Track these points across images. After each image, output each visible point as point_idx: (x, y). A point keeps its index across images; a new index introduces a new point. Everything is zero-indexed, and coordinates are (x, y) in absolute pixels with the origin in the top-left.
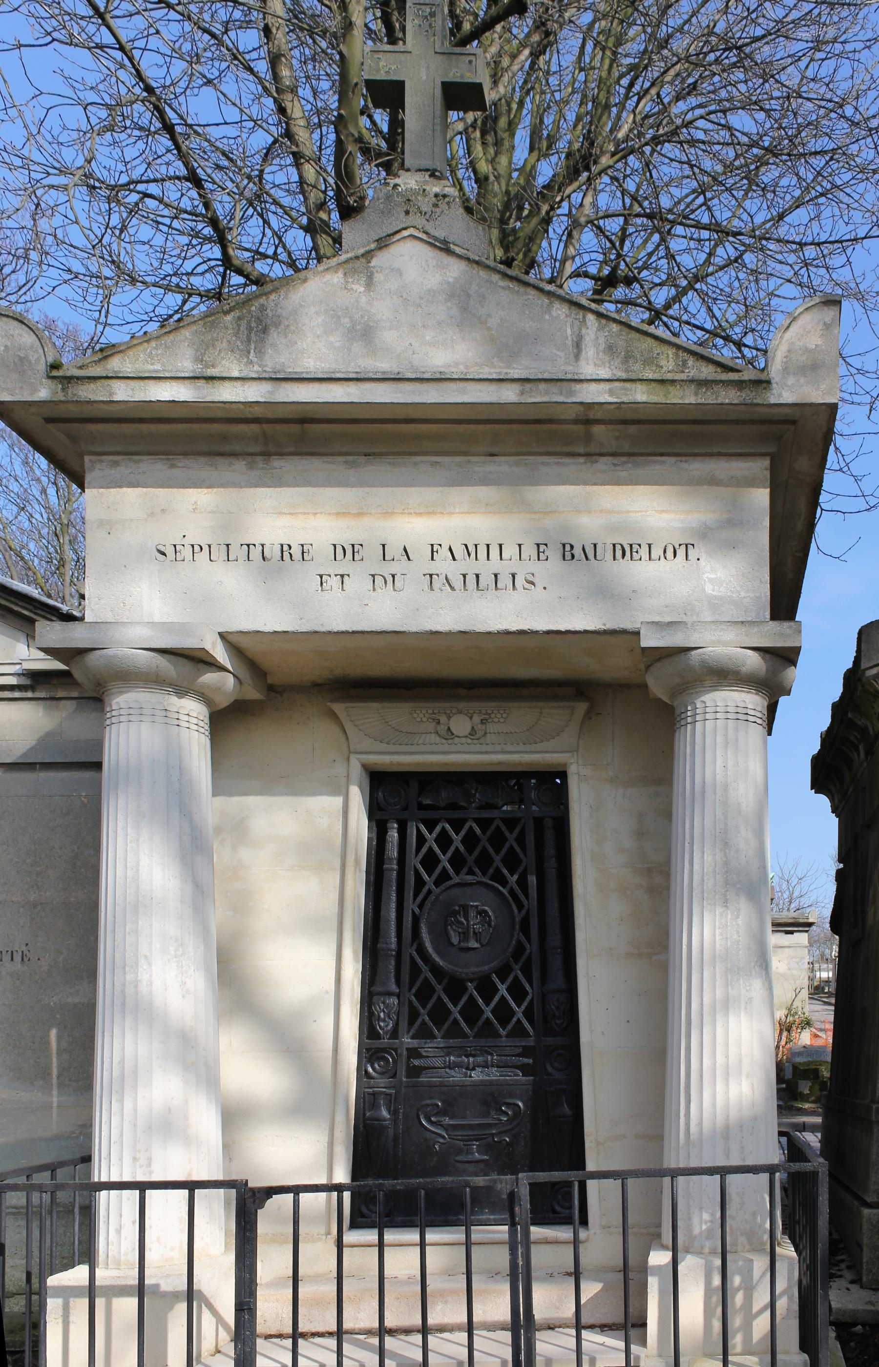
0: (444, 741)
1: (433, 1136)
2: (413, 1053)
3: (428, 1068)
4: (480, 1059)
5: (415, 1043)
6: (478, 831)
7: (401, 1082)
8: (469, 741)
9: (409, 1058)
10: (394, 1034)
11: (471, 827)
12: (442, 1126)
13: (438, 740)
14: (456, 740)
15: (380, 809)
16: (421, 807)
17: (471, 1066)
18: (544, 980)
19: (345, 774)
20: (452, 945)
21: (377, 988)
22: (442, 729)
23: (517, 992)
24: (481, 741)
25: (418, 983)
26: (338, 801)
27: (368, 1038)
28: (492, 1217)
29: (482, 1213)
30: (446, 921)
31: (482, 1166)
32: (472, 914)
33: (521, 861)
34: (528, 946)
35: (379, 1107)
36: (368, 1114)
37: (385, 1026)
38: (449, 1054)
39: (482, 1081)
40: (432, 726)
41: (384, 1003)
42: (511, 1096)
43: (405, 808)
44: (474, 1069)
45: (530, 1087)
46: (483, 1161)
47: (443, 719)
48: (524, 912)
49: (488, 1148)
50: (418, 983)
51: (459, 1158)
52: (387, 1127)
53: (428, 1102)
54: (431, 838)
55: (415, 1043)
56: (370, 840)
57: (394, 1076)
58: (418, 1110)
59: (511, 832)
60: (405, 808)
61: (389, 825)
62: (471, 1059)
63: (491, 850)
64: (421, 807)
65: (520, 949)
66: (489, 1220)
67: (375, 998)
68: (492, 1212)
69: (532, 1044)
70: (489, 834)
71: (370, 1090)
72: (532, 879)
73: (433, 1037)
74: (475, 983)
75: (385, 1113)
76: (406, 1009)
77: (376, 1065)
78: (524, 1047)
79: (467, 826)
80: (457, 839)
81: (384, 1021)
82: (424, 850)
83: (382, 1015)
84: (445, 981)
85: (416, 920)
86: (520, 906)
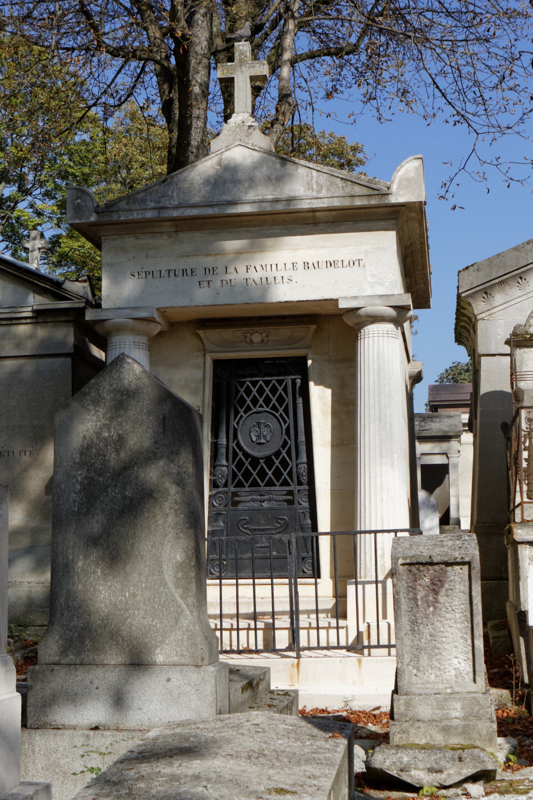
2: (235, 494)
4: (266, 497)
20: (253, 441)
22: (248, 340)
32: (262, 426)
34: (289, 441)
38: (251, 495)
44: (264, 502)
47: (249, 335)
48: (287, 425)
51: (257, 545)
53: (243, 518)
65: (285, 443)
84: (250, 459)
86: (285, 422)
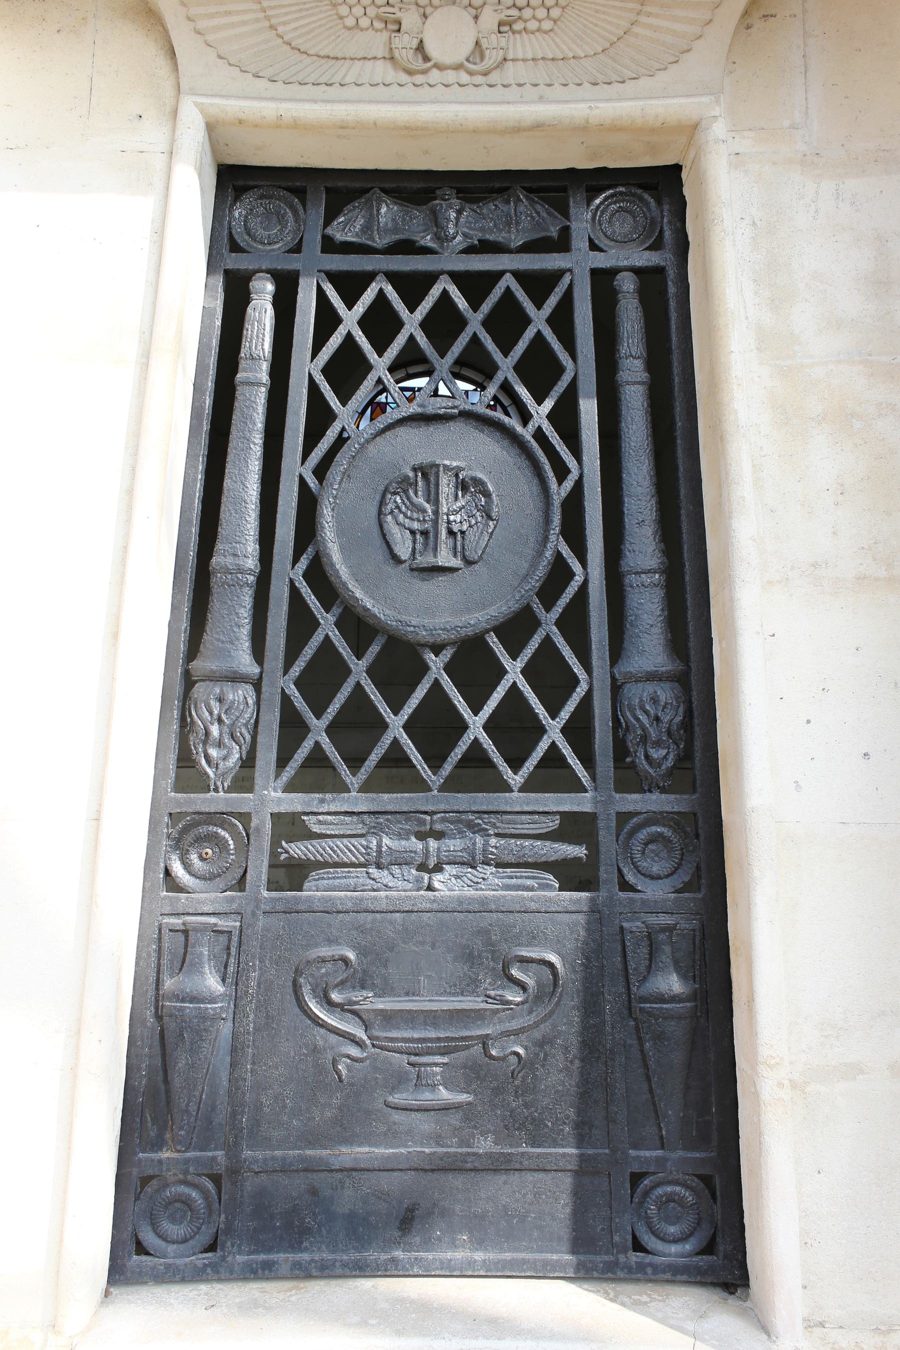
0: (404, 78)
1: (333, 1038)
2: (290, 826)
3: (326, 865)
4: (453, 845)
5: (295, 802)
6: (462, 303)
7: (258, 901)
8: (464, 78)
9: (275, 843)
10: (244, 778)
11: (445, 292)
12: (355, 1013)
13: (392, 75)
14: (435, 76)
15: (235, 247)
16: (329, 246)
17: (432, 863)
18: (617, 650)
19: (164, 147)
20: (397, 560)
21: (199, 665)
22: (405, 43)
23: (550, 677)
24: (494, 77)
25: (309, 652)
26: (148, 204)
27: (178, 788)
28: (479, 1256)
29: (454, 1245)
30: (382, 503)
31: (455, 1119)
32: (446, 486)
33: (560, 370)
34: (576, 567)
35: (197, 968)
36: (169, 984)
37: (221, 758)
38: (377, 830)
39: (460, 901)
40: (377, 42)
41: (220, 700)
42: (533, 939)
43: (297, 249)
44: (438, 868)
45: (581, 918)
46: (457, 1107)
47: (410, 19)
48: (569, 484)
49: (473, 1075)
50: (309, 652)
51: (397, 1098)
52: (216, 1018)
53: (325, 951)
54: (350, 319)
55: (295, 802)
56: (207, 312)
57: (241, 884)
58: (298, 972)
59: (539, 306)
60: (297, 249)
61: (255, 284)
62: (433, 844)
63: (490, 345)
64: (329, 246)
65: (559, 573)
66: (471, 1264)
67: (199, 690)
68: (479, 1243)
69: (587, 808)
70: (486, 307)
71: (176, 921)
72: (589, 409)
73: (344, 788)
74: (447, 654)
75: (212, 983)
76: (272, 718)
77: (194, 857)
78: (565, 816)
79: (435, 292)
80: (412, 322)
81: (220, 744)
82: (335, 341)
83: (215, 730)
84: (374, 649)
85: (308, 505)
86: (562, 472)
